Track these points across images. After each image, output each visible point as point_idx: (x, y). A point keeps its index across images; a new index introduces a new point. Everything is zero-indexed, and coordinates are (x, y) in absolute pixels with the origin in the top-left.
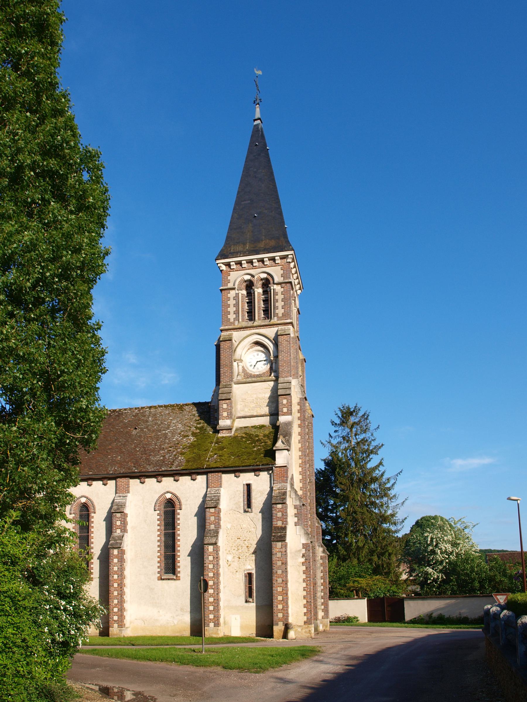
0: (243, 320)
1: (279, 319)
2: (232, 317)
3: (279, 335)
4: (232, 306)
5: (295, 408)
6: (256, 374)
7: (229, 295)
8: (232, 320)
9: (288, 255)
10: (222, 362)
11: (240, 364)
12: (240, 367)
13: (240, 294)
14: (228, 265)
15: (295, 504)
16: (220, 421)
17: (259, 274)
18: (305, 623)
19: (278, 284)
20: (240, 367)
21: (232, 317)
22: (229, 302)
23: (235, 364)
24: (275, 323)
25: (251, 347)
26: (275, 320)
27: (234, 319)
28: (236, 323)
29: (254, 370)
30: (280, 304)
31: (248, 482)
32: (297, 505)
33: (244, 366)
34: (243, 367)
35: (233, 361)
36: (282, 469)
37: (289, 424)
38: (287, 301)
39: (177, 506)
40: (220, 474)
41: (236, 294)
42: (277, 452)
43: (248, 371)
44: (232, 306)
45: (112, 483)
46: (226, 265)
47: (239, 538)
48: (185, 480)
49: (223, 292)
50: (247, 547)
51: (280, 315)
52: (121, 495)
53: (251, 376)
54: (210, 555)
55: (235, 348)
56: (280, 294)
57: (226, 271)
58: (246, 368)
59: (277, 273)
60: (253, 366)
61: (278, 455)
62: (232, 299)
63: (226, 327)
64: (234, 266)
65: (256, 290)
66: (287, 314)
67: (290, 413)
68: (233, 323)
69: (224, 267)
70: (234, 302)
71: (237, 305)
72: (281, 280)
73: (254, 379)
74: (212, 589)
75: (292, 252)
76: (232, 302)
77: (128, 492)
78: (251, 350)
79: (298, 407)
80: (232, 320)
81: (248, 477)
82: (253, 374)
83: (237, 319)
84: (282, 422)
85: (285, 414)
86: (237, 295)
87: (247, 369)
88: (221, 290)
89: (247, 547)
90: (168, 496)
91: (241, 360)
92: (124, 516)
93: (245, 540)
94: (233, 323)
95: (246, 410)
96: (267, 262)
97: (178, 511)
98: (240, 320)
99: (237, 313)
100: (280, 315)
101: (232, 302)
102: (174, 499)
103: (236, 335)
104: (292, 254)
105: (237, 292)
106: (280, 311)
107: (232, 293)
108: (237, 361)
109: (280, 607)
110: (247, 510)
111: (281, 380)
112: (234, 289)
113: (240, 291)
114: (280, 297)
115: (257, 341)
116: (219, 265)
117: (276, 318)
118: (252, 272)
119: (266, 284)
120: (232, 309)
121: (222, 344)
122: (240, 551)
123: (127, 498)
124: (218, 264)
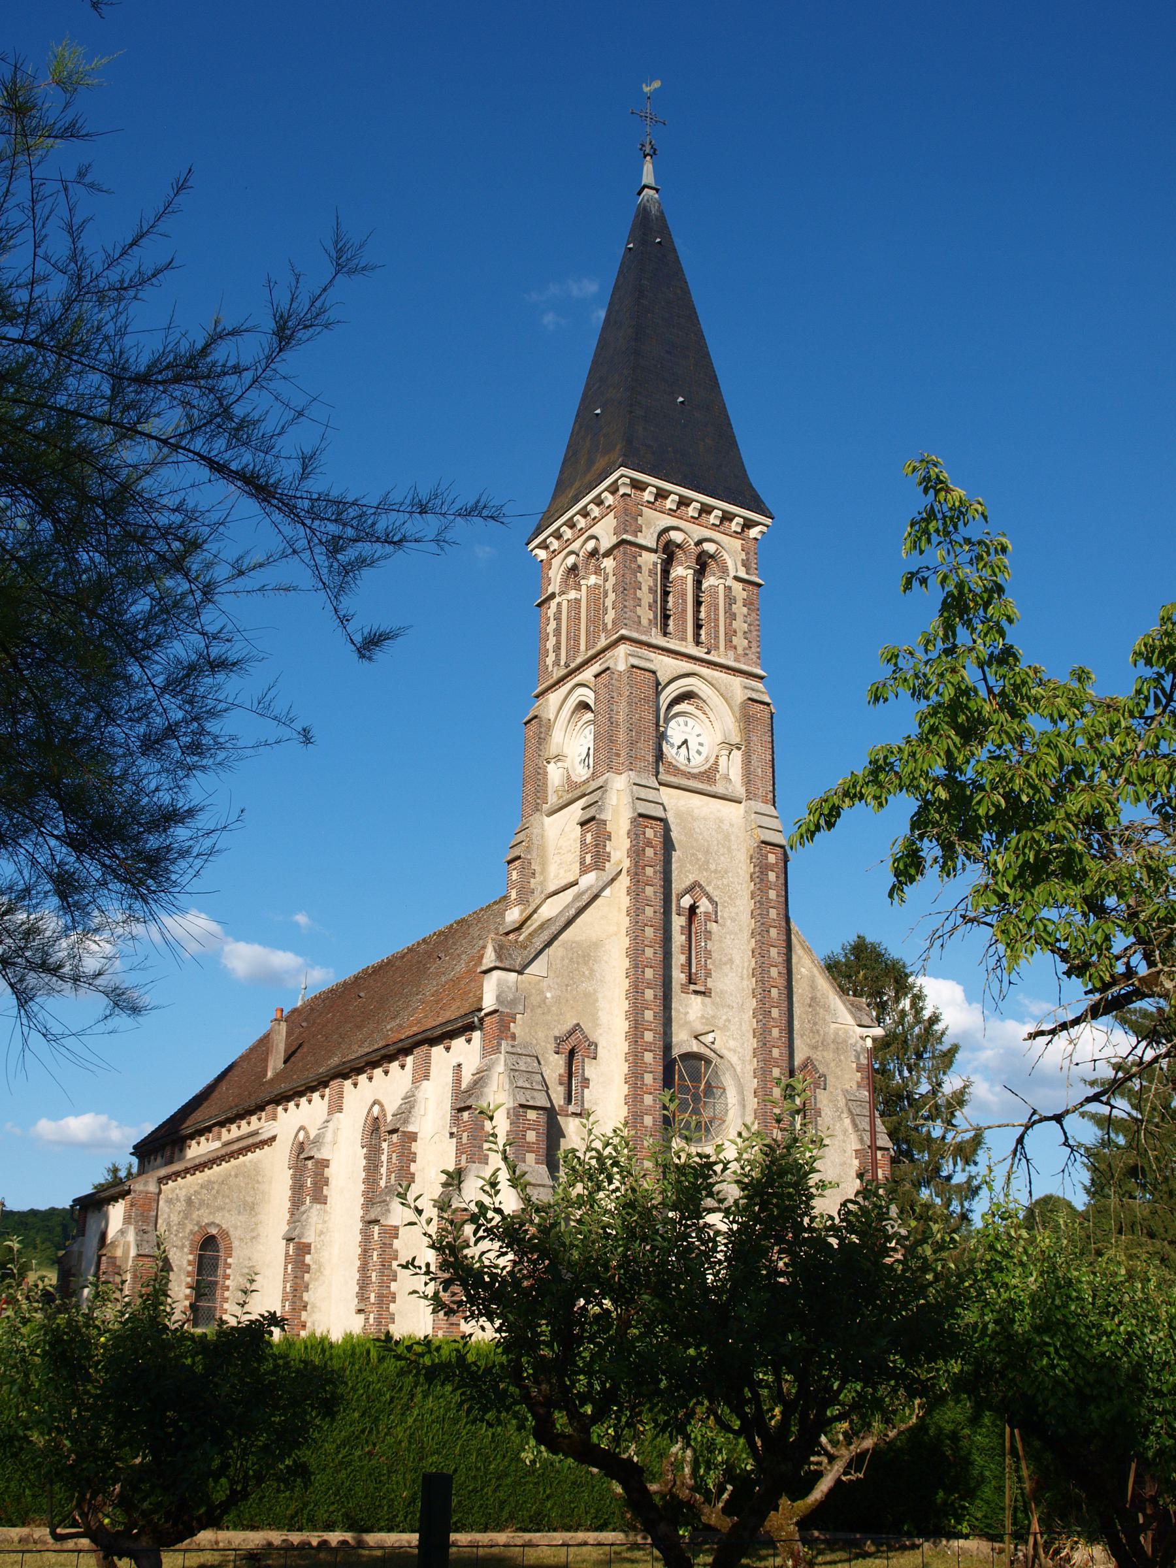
23: (551, 768)
51: (610, 626)
53: (577, 786)
69: (542, 554)
71: (557, 632)
77: (340, 1110)
78: (580, 724)
79: (626, 843)
83: (557, 663)
88: (539, 605)
107: (553, 604)
112: (553, 596)
113: (564, 597)
118: (575, 546)
120: (551, 644)
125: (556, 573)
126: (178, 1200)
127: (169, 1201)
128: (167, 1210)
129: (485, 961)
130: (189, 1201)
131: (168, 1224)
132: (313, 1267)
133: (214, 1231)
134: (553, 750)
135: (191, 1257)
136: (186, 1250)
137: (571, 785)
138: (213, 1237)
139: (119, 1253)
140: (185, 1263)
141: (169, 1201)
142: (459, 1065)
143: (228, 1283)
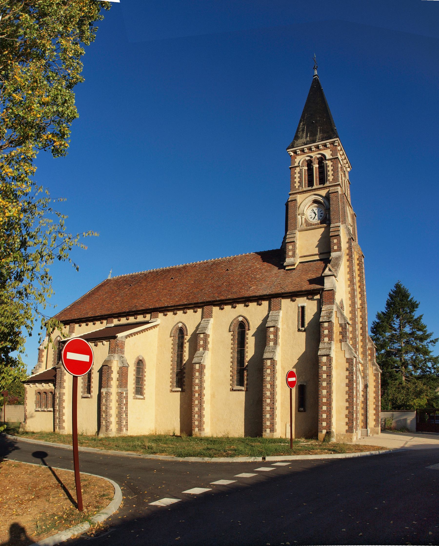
0: (305, 187)
1: (330, 183)
2: (297, 185)
3: (330, 193)
4: (297, 178)
5: (344, 245)
6: (315, 223)
7: (295, 171)
8: (297, 187)
9: (335, 141)
10: (289, 216)
11: (302, 217)
12: (303, 219)
13: (303, 170)
14: (295, 152)
15: (341, 323)
16: (286, 259)
17: (315, 155)
18: (347, 431)
19: (328, 160)
20: (303, 219)
21: (297, 185)
22: (295, 176)
23: (299, 217)
24: (327, 185)
25: (311, 205)
26: (327, 184)
27: (299, 186)
28: (301, 188)
29: (313, 221)
30: (330, 173)
31: (302, 305)
32: (342, 324)
33: (306, 218)
34: (305, 219)
35: (297, 215)
36: (330, 292)
37: (338, 258)
38: (335, 170)
39: (247, 328)
40: (279, 299)
41: (300, 169)
42: (325, 278)
43: (309, 222)
44: (297, 178)
45: (200, 310)
46: (293, 152)
48: (253, 305)
49: (292, 169)
51: (331, 180)
52: (206, 319)
53: (311, 225)
54: (268, 369)
55: (298, 206)
56: (330, 166)
57: (294, 156)
59: (328, 154)
60: (312, 219)
61: (326, 280)
62: (297, 173)
63: (293, 192)
64: (299, 152)
65: (314, 165)
66: (336, 179)
67: (339, 249)
68: (298, 189)
70: (299, 175)
71: (300, 177)
72: (331, 157)
73: (313, 227)
74: (269, 398)
75: (338, 139)
76: (297, 175)
77: (211, 317)
78: (311, 206)
81: (302, 301)
82: (313, 223)
84: (333, 257)
85: (335, 251)
86: (301, 170)
87: (308, 220)
90: (241, 319)
91: (303, 214)
92: (206, 336)
94: (298, 189)
96: (321, 147)
98: (303, 186)
99: (301, 182)
100: (331, 180)
101: (297, 175)
102: (245, 322)
103: (299, 198)
104: (337, 140)
105: (301, 168)
106: (331, 178)
107: (298, 170)
108: (300, 215)
109: (324, 416)
110: (301, 328)
111: (332, 225)
114: (330, 168)
115: (315, 199)
116: (289, 152)
117: (328, 182)
119: (322, 160)
120: (297, 180)
121: (289, 203)
123: (210, 322)
124: (288, 152)
125: (300, 159)
134: (300, 211)
137: (308, 223)
142: (303, 308)
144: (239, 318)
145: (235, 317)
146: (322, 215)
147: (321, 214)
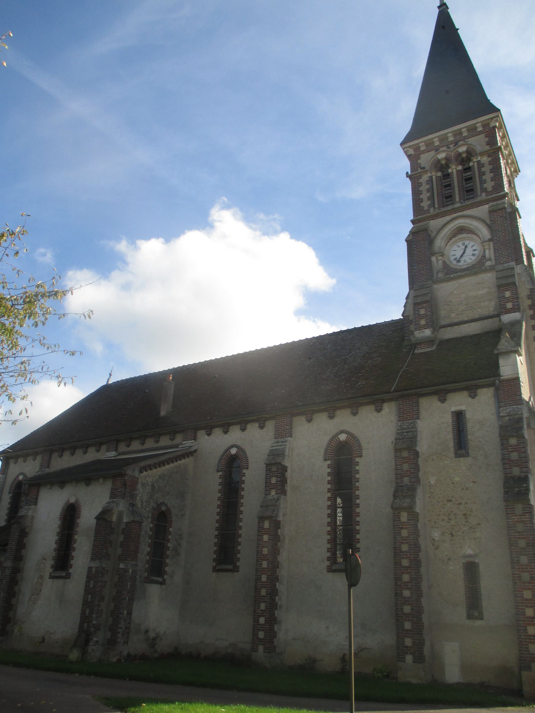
4: (424, 192)
6: (463, 267)
8: (426, 208)
23: (434, 259)
28: (432, 210)
34: (444, 262)
44: (424, 192)
47: (451, 501)
50: (465, 515)
58: (448, 263)
68: (428, 211)
80: (426, 208)
89: (465, 515)
93: (460, 504)
94: (428, 211)
95: (453, 315)
97: (357, 459)
99: (431, 198)
100: (489, 189)
122: (453, 522)
126: (148, 485)
127: (143, 485)
128: (141, 490)
129: (499, 347)
130: (153, 487)
131: (142, 501)
132: (281, 537)
133: (164, 508)
135: (152, 525)
136: (149, 520)
138: (163, 513)
139: (114, 518)
140: (149, 529)
141: (143, 485)
143: (169, 545)
144: (340, 436)
145: (334, 432)
146: (474, 252)
147: (474, 250)
